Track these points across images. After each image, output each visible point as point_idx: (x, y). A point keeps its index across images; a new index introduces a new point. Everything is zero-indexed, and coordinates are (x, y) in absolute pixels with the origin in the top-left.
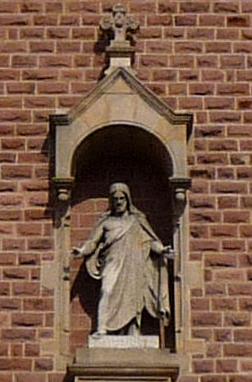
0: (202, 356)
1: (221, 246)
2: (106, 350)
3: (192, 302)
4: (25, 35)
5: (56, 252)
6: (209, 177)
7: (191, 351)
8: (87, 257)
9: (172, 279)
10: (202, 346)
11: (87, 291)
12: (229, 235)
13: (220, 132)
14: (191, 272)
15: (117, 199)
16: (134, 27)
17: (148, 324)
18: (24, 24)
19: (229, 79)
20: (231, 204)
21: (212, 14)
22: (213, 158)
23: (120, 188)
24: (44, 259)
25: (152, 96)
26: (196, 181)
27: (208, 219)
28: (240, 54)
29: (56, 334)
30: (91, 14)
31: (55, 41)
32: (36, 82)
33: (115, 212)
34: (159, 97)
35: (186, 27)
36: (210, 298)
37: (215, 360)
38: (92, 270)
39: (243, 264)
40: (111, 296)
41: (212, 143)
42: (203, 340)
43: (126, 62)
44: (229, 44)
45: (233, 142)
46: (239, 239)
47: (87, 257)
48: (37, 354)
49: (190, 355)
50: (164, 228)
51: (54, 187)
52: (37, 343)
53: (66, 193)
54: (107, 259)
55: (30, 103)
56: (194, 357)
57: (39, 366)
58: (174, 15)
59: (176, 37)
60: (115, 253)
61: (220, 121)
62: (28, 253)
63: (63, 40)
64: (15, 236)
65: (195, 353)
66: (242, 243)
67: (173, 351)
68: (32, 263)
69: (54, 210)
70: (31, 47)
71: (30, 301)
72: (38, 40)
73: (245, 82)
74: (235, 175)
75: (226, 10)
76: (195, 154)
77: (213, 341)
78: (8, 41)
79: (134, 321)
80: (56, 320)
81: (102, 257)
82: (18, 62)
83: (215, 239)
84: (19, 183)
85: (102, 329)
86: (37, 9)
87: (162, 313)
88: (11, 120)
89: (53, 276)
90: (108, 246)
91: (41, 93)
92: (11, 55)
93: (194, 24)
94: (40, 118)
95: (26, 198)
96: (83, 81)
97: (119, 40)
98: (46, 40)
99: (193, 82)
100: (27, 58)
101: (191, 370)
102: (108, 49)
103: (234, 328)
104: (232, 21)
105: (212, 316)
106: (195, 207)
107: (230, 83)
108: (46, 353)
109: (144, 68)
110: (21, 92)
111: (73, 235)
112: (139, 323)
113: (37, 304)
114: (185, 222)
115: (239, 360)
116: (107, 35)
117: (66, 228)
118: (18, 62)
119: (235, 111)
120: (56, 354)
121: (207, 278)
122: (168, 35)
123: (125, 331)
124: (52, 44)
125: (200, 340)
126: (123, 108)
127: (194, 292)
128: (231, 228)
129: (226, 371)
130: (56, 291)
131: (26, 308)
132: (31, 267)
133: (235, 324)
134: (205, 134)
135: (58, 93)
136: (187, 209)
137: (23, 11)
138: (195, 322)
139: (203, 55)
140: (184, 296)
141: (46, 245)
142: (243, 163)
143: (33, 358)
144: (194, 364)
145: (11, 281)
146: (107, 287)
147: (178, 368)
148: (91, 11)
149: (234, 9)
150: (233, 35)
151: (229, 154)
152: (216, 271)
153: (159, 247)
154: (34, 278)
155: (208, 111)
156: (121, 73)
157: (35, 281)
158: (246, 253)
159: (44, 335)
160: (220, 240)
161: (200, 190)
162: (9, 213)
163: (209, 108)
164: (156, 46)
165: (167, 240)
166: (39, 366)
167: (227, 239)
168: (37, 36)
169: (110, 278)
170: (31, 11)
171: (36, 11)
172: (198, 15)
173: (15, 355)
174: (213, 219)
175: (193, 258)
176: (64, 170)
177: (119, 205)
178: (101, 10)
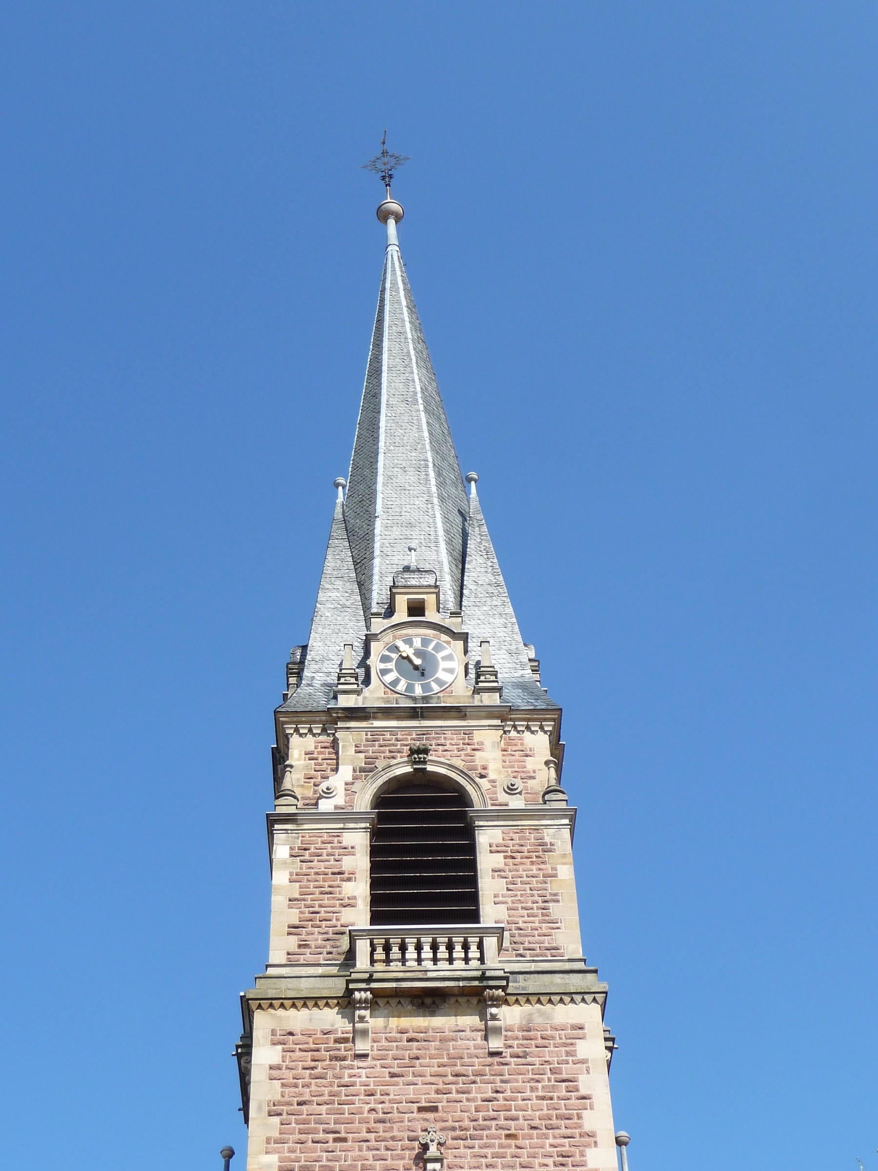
4: (369, 1149)
16: (442, 1141)
18: (368, 1141)
21: (494, 1131)
30: (413, 1133)
31: (389, 1153)
63: (394, 1152)
72: (378, 1152)
75: (503, 1129)
92: (360, 1163)
97: (433, 1151)
98: (383, 1152)
102: (425, 1157)
104: (508, 1136)
116: (425, 1147)
122: (465, 1147)
137: (367, 1132)
139: (489, 1160)
150: (509, 1146)
168: (378, 1149)
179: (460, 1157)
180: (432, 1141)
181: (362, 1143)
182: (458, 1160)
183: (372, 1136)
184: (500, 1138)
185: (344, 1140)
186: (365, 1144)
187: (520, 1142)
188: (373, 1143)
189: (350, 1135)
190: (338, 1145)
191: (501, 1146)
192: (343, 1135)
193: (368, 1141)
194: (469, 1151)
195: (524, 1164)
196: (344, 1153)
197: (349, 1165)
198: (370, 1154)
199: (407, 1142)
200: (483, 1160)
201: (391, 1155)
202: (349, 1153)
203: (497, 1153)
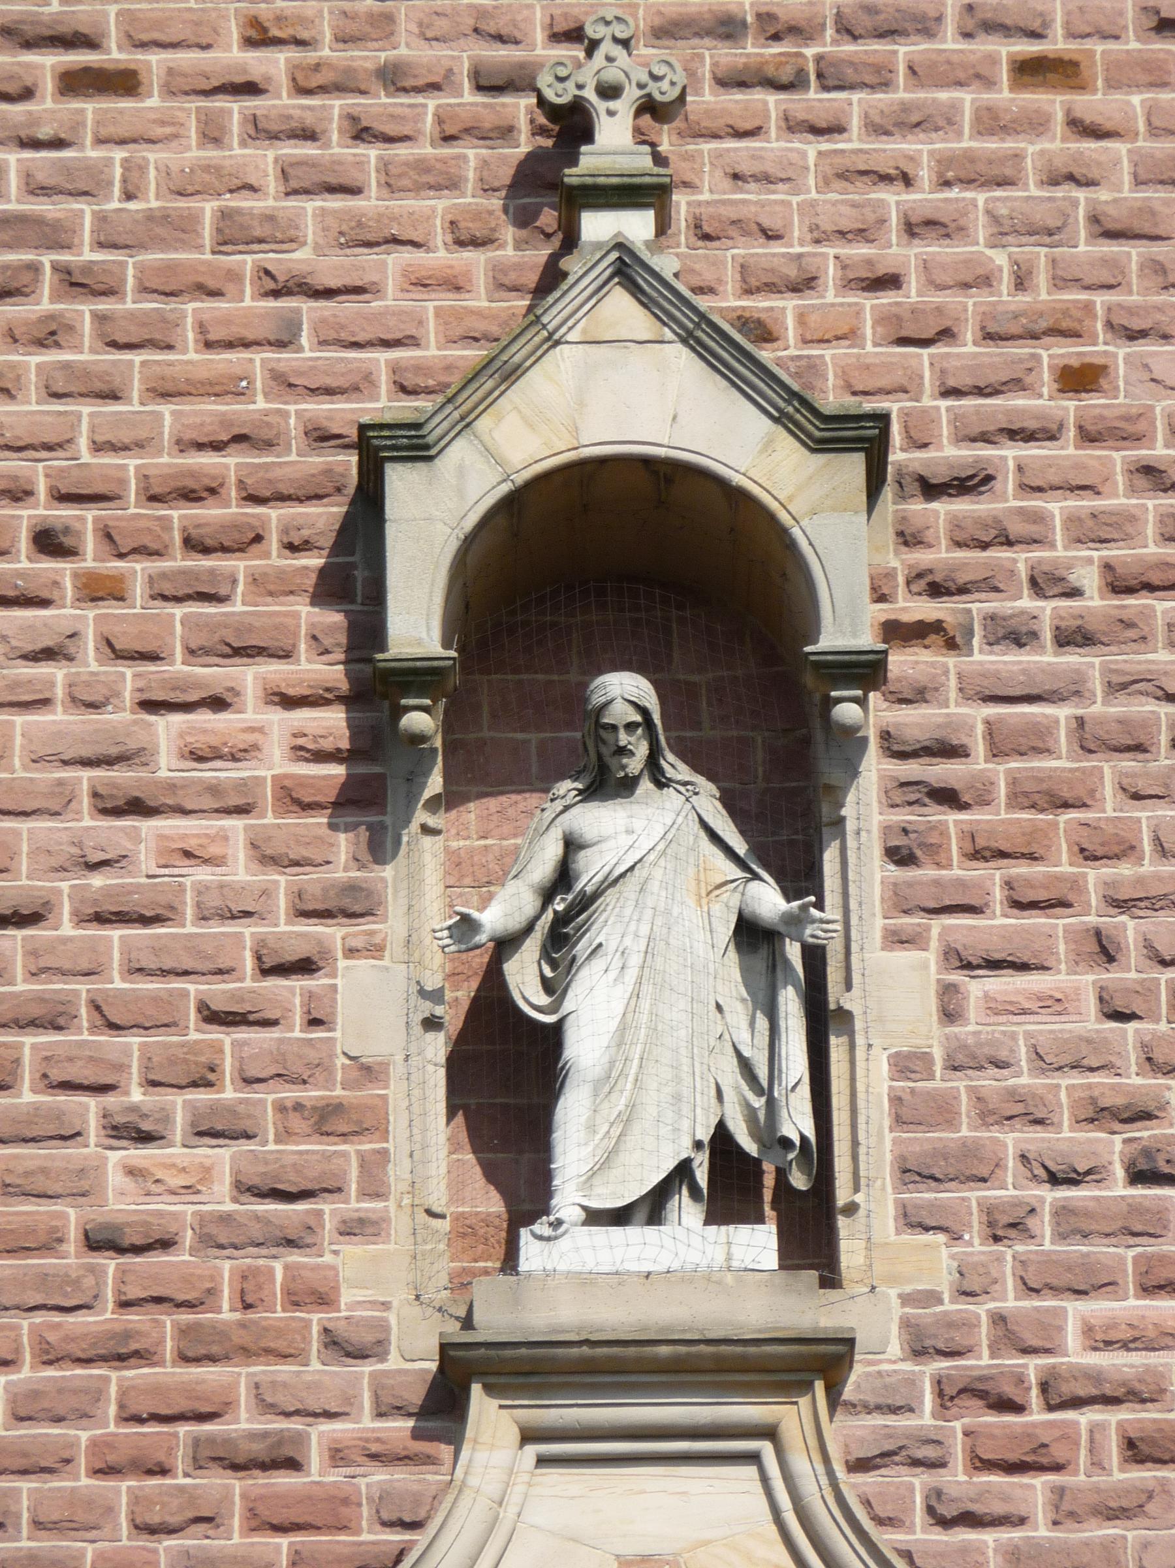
0: (933, 1298)
1: (998, 894)
2: (585, 1281)
3: (896, 1100)
4: (260, 131)
5: (392, 925)
6: (951, 645)
7: (892, 1280)
8: (505, 945)
9: (822, 1021)
10: (935, 1262)
11: (506, 1073)
12: (1032, 857)
13: (989, 479)
14: (893, 991)
15: (614, 728)
16: (665, 92)
17: (729, 1179)
18: (251, 89)
19: (1021, 282)
20: (1035, 742)
21: (950, 42)
22: (962, 578)
23: (624, 690)
24: (351, 952)
25: (730, 351)
26: (904, 663)
27: (947, 797)
28: (1059, 192)
29: (400, 1223)
31: (372, 153)
32: (306, 307)
33: (605, 783)
34: (765, 355)
35: (856, 96)
36: (960, 1083)
37: (982, 1310)
38: (524, 978)
39: (1078, 961)
40: (606, 1084)
41: (956, 524)
42: (941, 1238)
43: (636, 226)
44: (1018, 156)
45: (1039, 518)
46: (1066, 869)
47: (505, 945)
48: (324, 1299)
49: (893, 1293)
50: (785, 828)
51: (376, 687)
52: (328, 1258)
53: (425, 709)
54: (582, 948)
55: (284, 383)
56: (906, 1299)
57: (341, 1347)
58: (810, 52)
59: (817, 131)
60: (611, 929)
61: (985, 438)
62: (290, 934)
63: (402, 151)
64: (241, 871)
65: (908, 1289)
66: (1077, 884)
67: (830, 1279)
68: (305, 966)
69: (371, 792)
70: (284, 174)
71: (298, 1107)
72: (308, 150)
73: (1083, 296)
74: (1047, 636)
76: (898, 562)
77: (976, 1245)
78: (194, 153)
79: (683, 1170)
80: (398, 1173)
81: (561, 941)
82: (233, 233)
83: (979, 872)
84: (250, 677)
85: (568, 1198)
86: (305, 35)
87: (786, 1143)
88: (217, 446)
89: (384, 1012)
90: (586, 902)
91: (323, 343)
92: (208, 208)
93: (885, 85)
94: (321, 437)
95: (283, 734)
96: (479, 300)
97: (614, 144)
98: (336, 148)
99: (887, 298)
100: (269, 218)
101: (895, 1348)
103: (1051, 1196)
104: (1030, 70)
105: (970, 1151)
106: (902, 755)
107: (1024, 298)
108: (360, 1295)
109: (704, 251)
110: (246, 344)
111: (455, 864)
112: (702, 1177)
113: (326, 1120)
114: (867, 804)
115: (1075, 1310)
116: (571, 125)
117: (427, 841)
118: (233, 233)
119: (1043, 401)
120: (400, 1297)
121: (950, 1015)
122: (793, 126)
123: (653, 1207)
124: (360, 164)
125: (929, 1237)
126: (617, 392)
127: (906, 1065)
128: (1034, 833)
129: (1027, 1351)
130: (397, 1070)
131: (284, 1135)
132: (298, 983)
133: (1054, 1179)
134: (931, 489)
135: (387, 344)
136: (874, 768)
137: (250, 43)
138: (911, 1173)
139: (924, 197)
140: (868, 1077)
141: (350, 906)
142: (1074, 593)
143: (316, 1318)
144: (906, 1324)
145: (226, 1038)
146: (583, 1050)
147: (850, 1342)
148: (500, 38)
149: (1036, 25)
150: (1036, 125)
151: (1021, 560)
152: (978, 988)
153: (768, 900)
154: (315, 1022)
155: (944, 404)
156: (627, 269)
157: (318, 1034)
158: (1092, 919)
159: (351, 1229)
160: (992, 878)
161: (918, 695)
162: (214, 789)
163: (949, 392)
164: (745, 168)
165: (800, 875)
166: (341, 1347)
167: (1020, 869)
168: (308, 135)
169: (594, 1017)
170: (278, 42)
171: (300, 43)
172: (902, 50)
173: (247, 1306)
174: (966, 798)
175: (898, 940)
176: (416, 624)
177: (622, 751)
178: (540, 36)
179: (766, 179)
180: (609, 92)
181: (220, 103)
182: (751, 194)
183: (275, 64)
184: (987, 82)
185: (124, 82)
186: (235, 108)
187: (1095, 103)
188: (281, 102)
189: (155, 58)
190: (90, 108)
191: (991, 123)
192: (114, 55)
193: (251, 89)
194: (811, 149)
195: (1116, 217)
196: (119, 154)
197: (150, 217)
198: (265, 160)
199: (469, 97)
200: (891, 198)
201: (385, 166)
202: (153, 155)
203: (969, 157)
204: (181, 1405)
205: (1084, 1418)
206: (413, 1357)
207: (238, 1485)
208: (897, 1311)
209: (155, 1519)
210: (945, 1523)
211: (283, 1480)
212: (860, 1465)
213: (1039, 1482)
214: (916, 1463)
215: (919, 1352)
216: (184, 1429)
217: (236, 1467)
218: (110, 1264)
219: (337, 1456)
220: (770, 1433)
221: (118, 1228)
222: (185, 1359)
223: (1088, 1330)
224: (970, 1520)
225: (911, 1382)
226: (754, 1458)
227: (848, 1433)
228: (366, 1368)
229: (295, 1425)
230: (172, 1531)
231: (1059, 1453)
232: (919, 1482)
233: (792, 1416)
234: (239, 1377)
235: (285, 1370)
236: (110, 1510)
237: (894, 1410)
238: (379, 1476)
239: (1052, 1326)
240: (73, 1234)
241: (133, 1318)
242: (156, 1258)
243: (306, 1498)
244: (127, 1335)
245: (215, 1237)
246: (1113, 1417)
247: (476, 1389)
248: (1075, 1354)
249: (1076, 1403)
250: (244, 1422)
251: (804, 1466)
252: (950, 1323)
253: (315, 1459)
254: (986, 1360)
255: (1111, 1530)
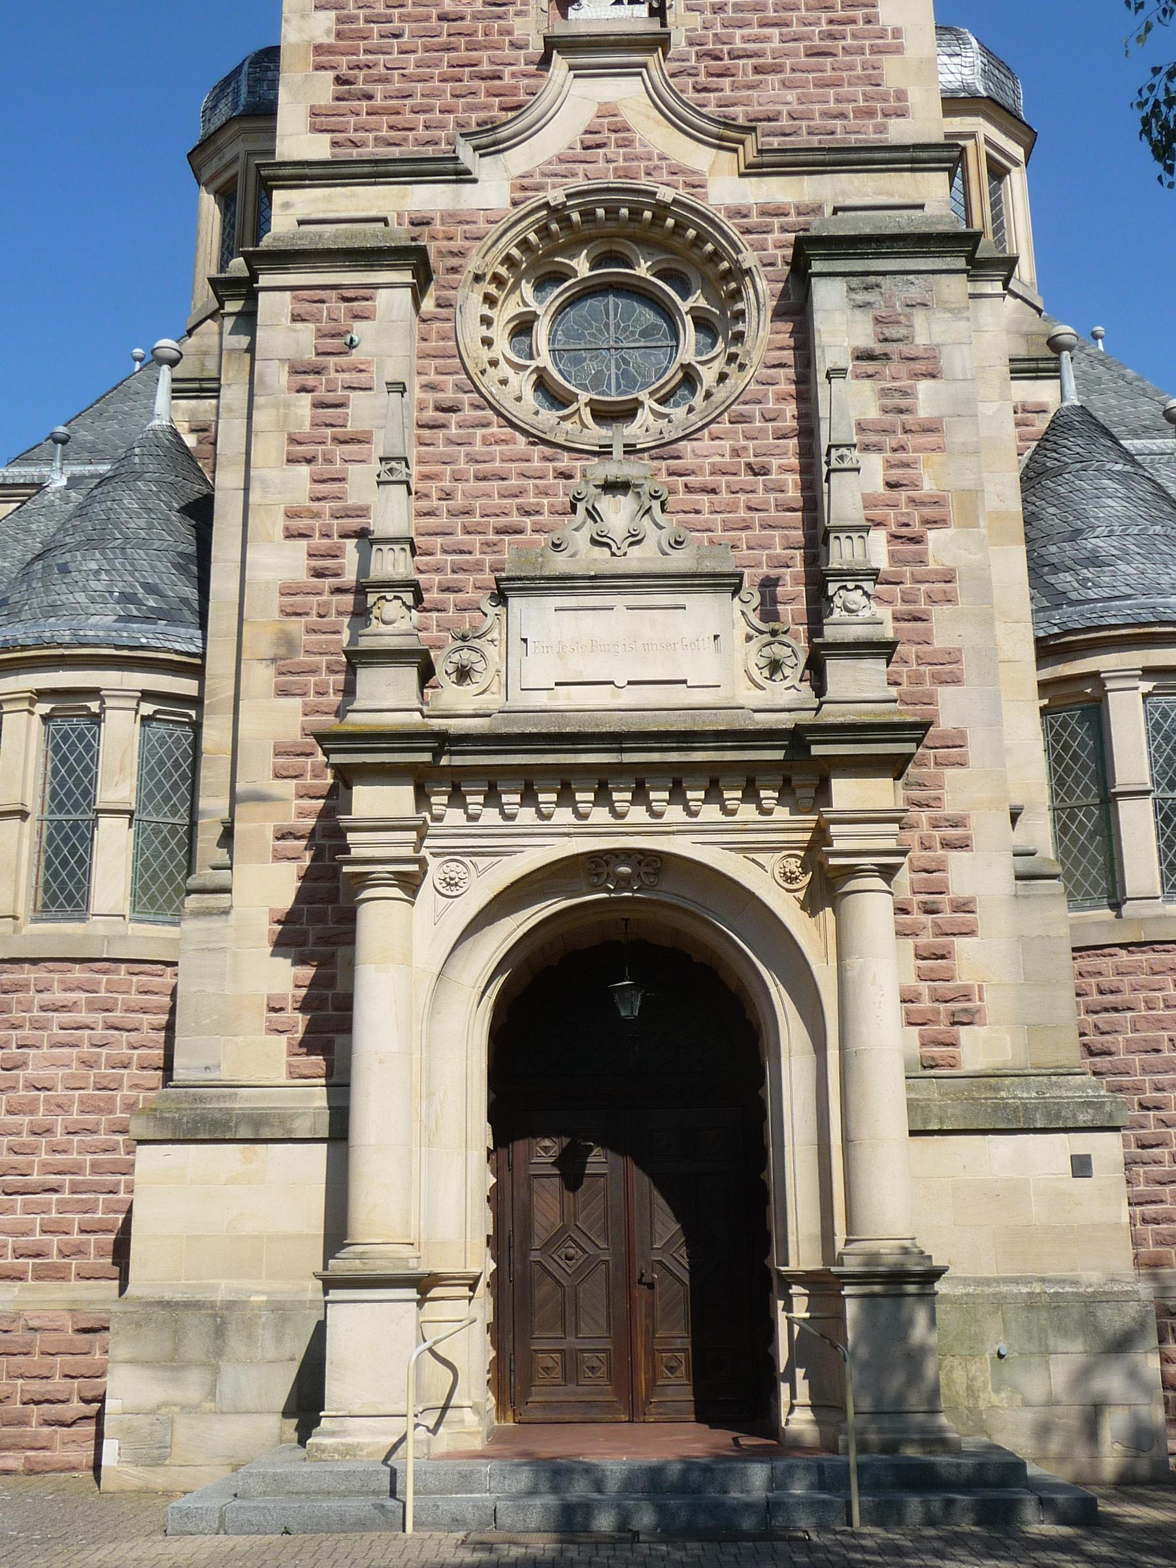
7: (682, 25)
10: (696, 20)
37: (710, 33)
48: (509, 33)
56: (687, 30)
57: (512, 44)
77: (708, 15)
101: (683, 44)
120: (533, 33)
129: (724, 43)
143: (507, 39)
144: (687, 37)
159: (518, 14)
204: (467, 62)
205: (741, 62)
206: (537, 47)
207: (483, 84)
208: (684, 33)
209: (458, 93)
210: (699, 91)
211: (497, 82)
212: (673, 75)
213: (728, 80)
214: (690, 75)
215: (691, 45)
216: (467, 69)
217: (482, 79)
218: (445, 25)
219: (513, 75)
220: (644, 65)
221: (447, 14)
222: (467, 50)
223: (743, 37)
224: (706, 90)
225: (689, 53)
226: (640, 74)
227: (668, 67)
228: (523, 52)
229: (501, 67)
230: (463, 97)
231: (733, 71)
232: (691, 80)
233: (652, 60)
234: (484, 55)
235: (498, 52)
236: (445, 91)
237: (683, 60)
238: (526, 81)
239: (732, 36)
240: (434, 16)
241: (452, 39)
242: (458, 23)
243: (504, 87)
244: (450, 43)
245: (476, 17)
246: (751, 62)
247: (555, 52)
248: (739, 44)
249: (739, 57)
250: (485, 67)
251: (655, 74)
252: (701, 36)
253: (507, 77)
254: (711, 47)
255: (749, 92)
